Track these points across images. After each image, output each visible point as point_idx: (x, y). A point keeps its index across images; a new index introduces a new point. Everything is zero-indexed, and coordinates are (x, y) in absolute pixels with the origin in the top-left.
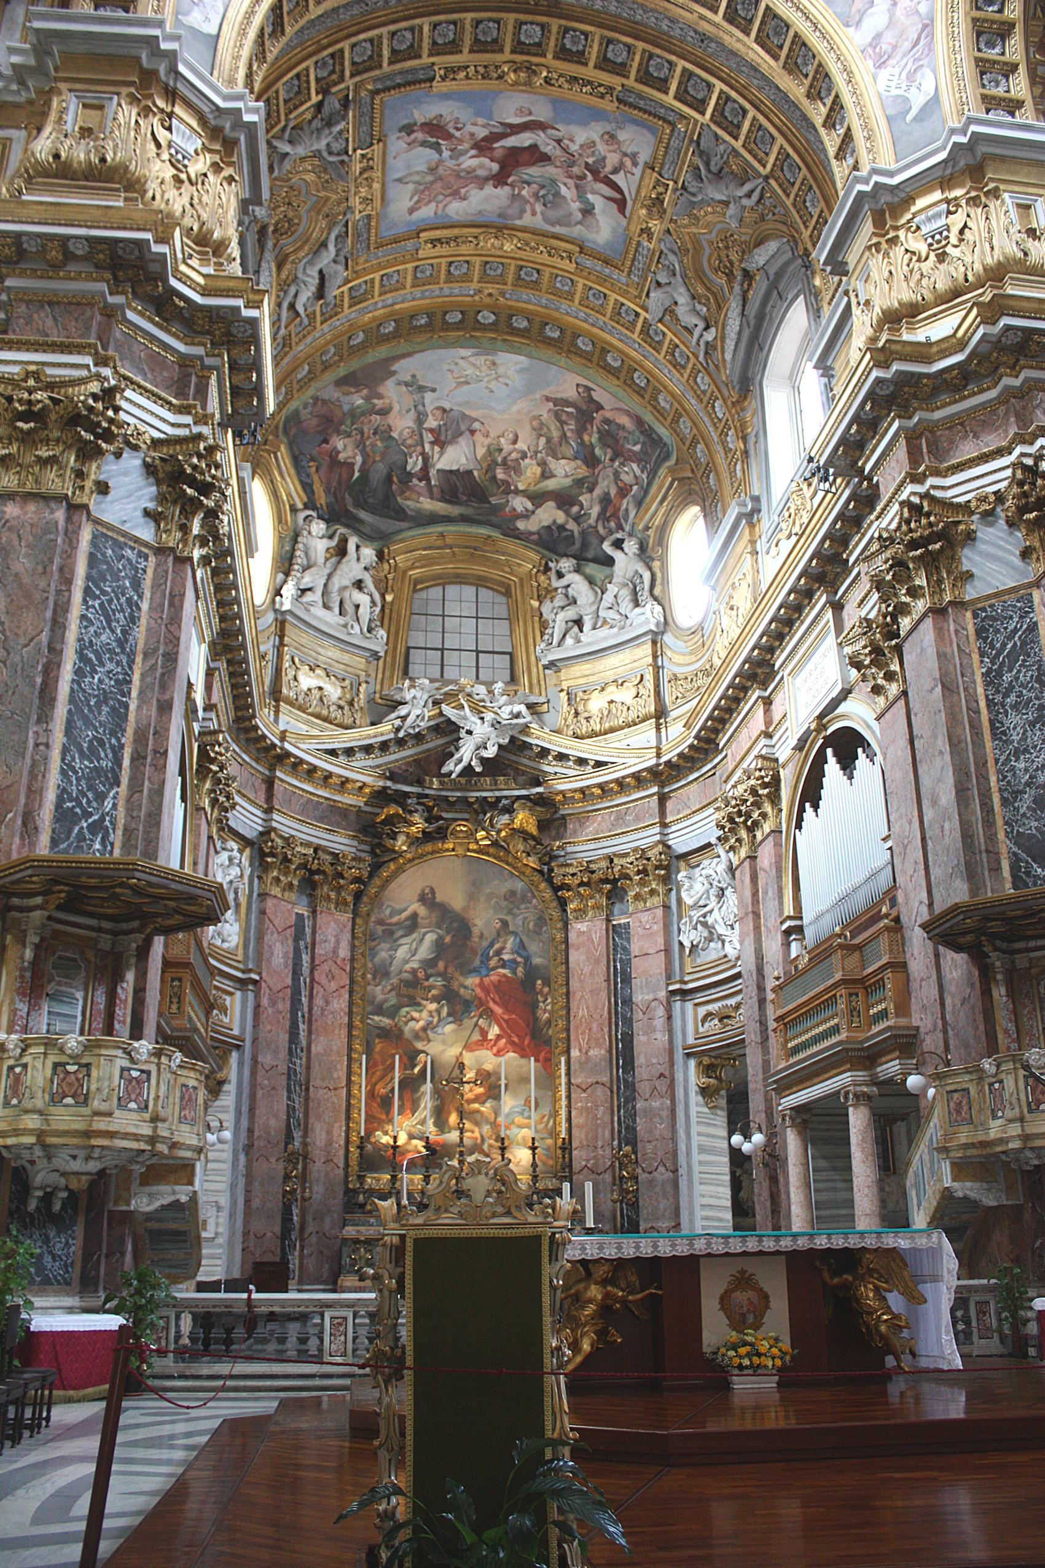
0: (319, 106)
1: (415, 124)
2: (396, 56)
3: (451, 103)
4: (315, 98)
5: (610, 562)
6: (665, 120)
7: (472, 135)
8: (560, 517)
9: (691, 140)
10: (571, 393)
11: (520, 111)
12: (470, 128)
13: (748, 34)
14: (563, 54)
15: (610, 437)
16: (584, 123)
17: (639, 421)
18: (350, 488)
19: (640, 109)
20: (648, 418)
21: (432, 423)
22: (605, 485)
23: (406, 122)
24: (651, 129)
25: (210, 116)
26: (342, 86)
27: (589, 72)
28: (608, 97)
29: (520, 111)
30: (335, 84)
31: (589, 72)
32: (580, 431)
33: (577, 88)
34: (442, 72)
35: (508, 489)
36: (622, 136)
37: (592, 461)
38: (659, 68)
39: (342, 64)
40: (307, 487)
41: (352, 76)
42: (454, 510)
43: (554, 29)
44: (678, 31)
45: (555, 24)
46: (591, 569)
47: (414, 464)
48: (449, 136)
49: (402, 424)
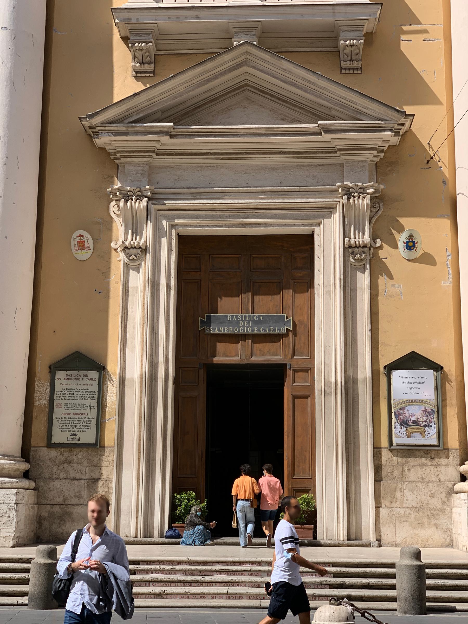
5: (431, 426)
8: (425, 423)
10: (424, 409)
15: (429, 413)
17: (431, 409)
18: (402, 422)
20: (432, 409)
21: (410, 415)
22: (429, 418)
32: (425, 413)
35: (419, 422)
37: (427, 416)
40: (397, 421)
42: (414, 424)
46: (430, 428)
47: (409, 420)
49: (407, 415)
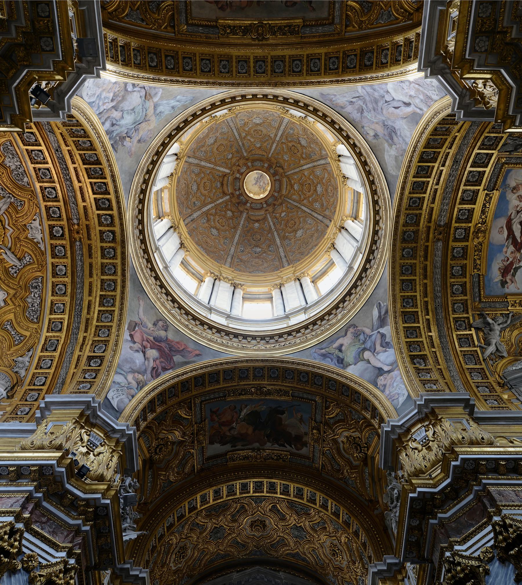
0: (477, 329)
1: (502, 280)
2: (464, 293)
3: (493, 265)
4: (473, 332)
6: (501, 168)
7: (512, 253)
9: (510, 154)
11: (501, 232)
12: (508, 254)
13: (440, 152)
14: (469, 220)
16: (508, 202)
19: (497, 180)
23: (499, 285)
24: (508, 172)
25: (421, 417)
26: (471, 318)
27: (478, 207)
28: (491, 195)
29: (501, 232)
30: (469, 321)
31: (478, 207)
33: (487, 210)
34: (476, 270)
36: (513, 184)
38: (473, 176)
39: (461, 318)
41: (468, 313)
43: (457, 225)
44: (454, 173)
45: (454, 224)
48: (512, 263)
